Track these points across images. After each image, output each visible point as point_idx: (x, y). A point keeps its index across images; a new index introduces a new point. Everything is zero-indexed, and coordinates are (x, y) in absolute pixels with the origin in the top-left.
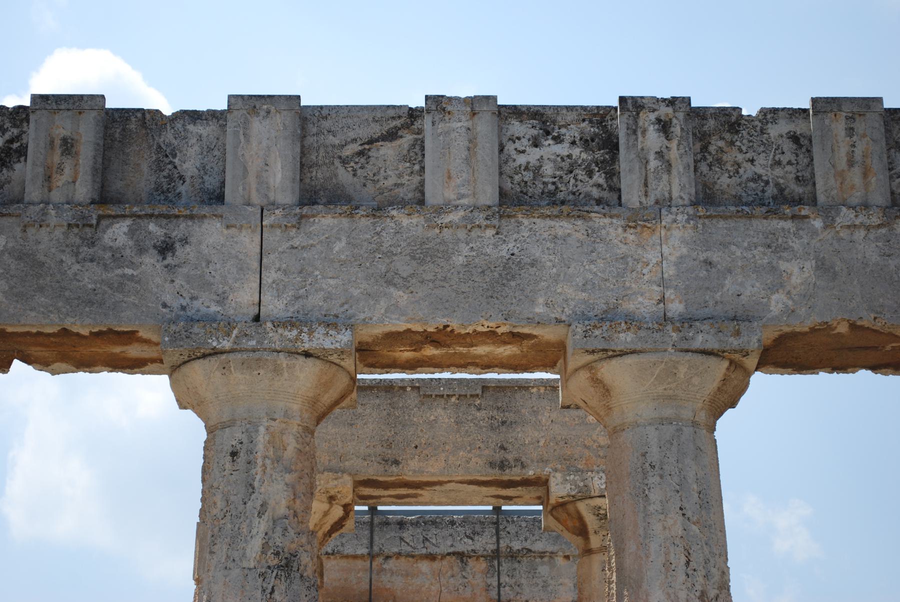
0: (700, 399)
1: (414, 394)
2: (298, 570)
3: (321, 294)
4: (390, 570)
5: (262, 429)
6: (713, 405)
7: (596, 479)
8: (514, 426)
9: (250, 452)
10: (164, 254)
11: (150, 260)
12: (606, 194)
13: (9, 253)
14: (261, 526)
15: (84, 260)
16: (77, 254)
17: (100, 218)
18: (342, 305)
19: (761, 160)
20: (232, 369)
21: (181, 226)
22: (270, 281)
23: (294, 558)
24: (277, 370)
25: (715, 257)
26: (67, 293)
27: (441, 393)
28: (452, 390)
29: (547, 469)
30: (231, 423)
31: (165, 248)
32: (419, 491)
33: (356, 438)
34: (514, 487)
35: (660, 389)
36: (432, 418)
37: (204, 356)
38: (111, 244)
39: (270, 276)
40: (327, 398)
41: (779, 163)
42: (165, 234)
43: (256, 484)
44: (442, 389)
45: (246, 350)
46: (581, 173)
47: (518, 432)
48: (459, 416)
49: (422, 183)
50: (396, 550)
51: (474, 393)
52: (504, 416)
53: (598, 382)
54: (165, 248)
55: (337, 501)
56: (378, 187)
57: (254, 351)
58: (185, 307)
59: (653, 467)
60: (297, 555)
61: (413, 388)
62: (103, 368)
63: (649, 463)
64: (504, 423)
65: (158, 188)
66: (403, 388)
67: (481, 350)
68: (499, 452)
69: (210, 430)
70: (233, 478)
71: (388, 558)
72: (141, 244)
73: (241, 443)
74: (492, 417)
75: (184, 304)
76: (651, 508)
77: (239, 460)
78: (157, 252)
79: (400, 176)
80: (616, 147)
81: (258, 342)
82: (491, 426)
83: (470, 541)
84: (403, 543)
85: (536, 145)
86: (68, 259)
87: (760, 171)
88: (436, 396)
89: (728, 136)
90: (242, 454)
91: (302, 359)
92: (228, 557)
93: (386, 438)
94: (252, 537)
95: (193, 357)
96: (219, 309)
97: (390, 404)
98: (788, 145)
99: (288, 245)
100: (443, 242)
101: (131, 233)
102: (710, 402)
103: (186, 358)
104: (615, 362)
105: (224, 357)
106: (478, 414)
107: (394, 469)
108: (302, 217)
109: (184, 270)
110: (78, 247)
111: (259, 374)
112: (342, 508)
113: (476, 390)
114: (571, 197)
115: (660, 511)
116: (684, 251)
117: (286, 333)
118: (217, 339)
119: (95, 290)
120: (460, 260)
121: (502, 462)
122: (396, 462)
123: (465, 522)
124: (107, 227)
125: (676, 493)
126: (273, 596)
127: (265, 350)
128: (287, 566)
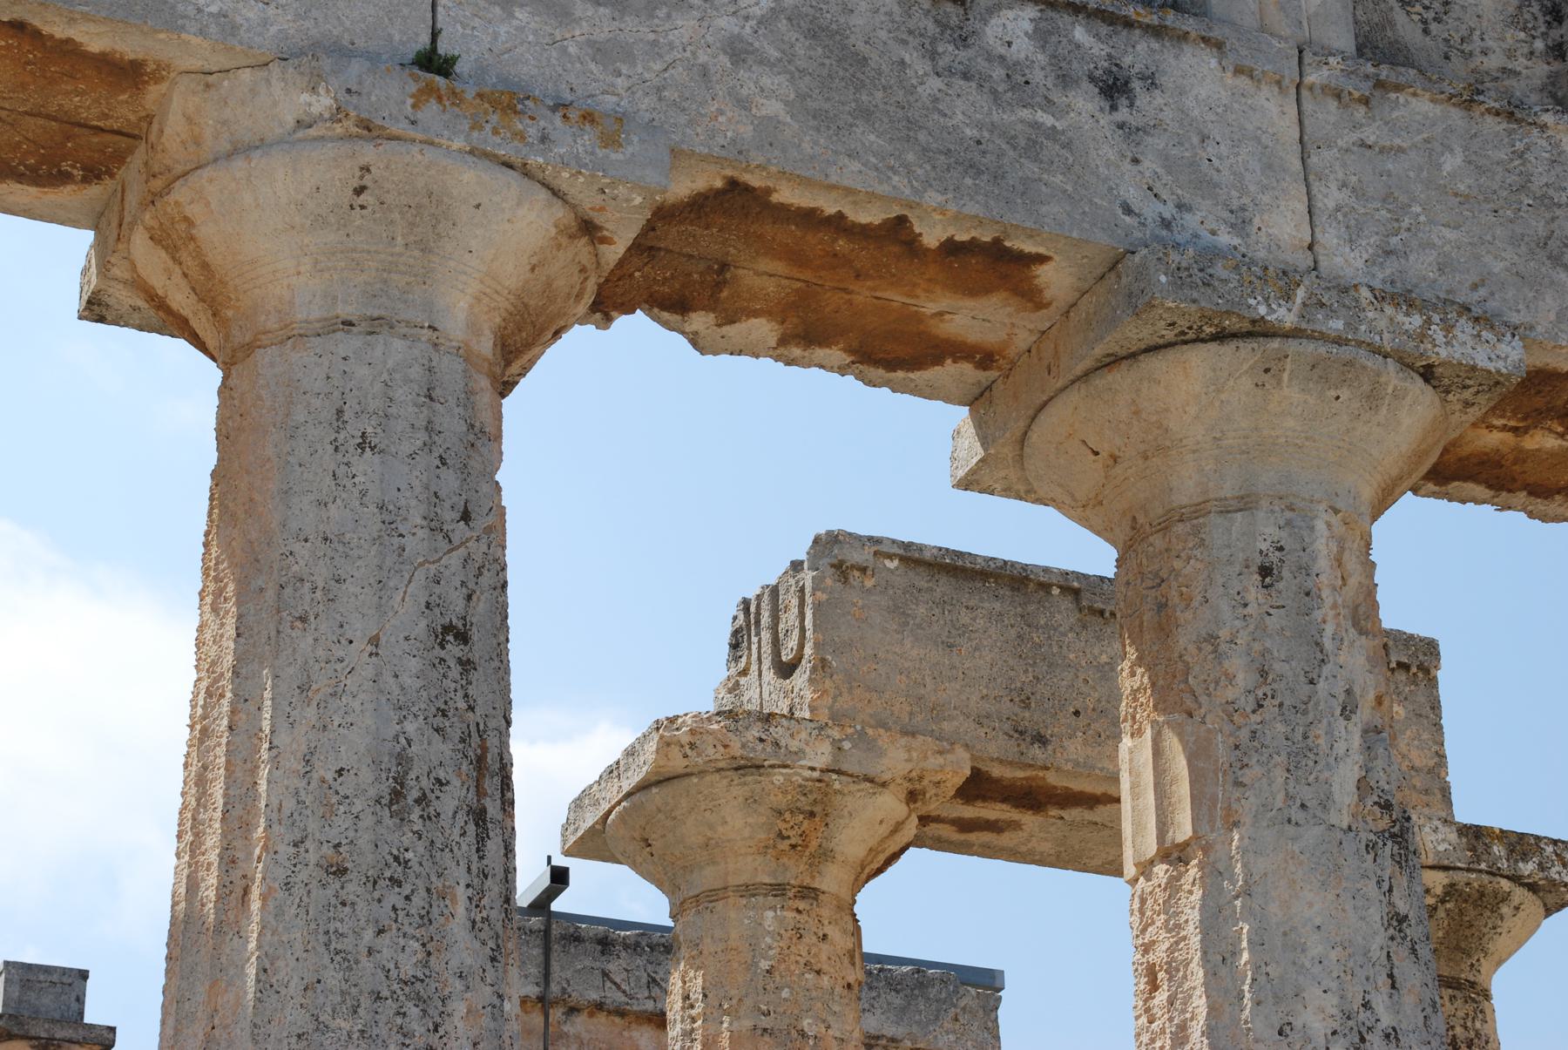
1: (1067, 603)
3: (1431, 256)
4: (578, 1037)
5: (1320, 525)
7: (1427, 829)
9: (1305, 570)
10: (1112, 97)
11: (1085, 103)
13: (789, 19)
15: (950, 71)
16: (933, 55)
18: (1475, 287)
20: (1286, 376)
21: (1139, 47)
22: (1331, 204)
24: (1373, 398)
26: (922, 136)
30: (1246, 503)
31: (1114, 88)
32: (1029, 819)
36: (1104, 658)
37: (1221, 337)
38: (1002, 50)
39: (1330, 197)
42: (1109, 56)
43: (1328, 644)
45: (1322, 337)
50: (594, 996)
56: (1472, 66)
57: (1339, 341)
58: (1170, 223)
61: (1066, 590)
66: (1045, 587)
70: (1273, 623)
71: (573, 1010)
72: (1063, 64)
73: (1281, 549)
75: (1167, 215)
77: (1281, 585)
78: (1097, 90)
79: (1510, 54)
81: (1347, 324)
84: (608, 984)
90: (1286, 573)
92: (1289, 797)
93: (1019, 685)
96: (1236, 241)
97: (1022, 616)
99: (1355, 136)
101: (1041, 36)
105: (1275, 344)
107: (1036, 751)
108: (1380, 84)
109: (1157, 142)
110: (934, 40)
111: (1338, 398)
117: (1400, 318)
118: (1267, 299)
119: (979, 142)
122: (1041, 740)
127: (1360, 344)
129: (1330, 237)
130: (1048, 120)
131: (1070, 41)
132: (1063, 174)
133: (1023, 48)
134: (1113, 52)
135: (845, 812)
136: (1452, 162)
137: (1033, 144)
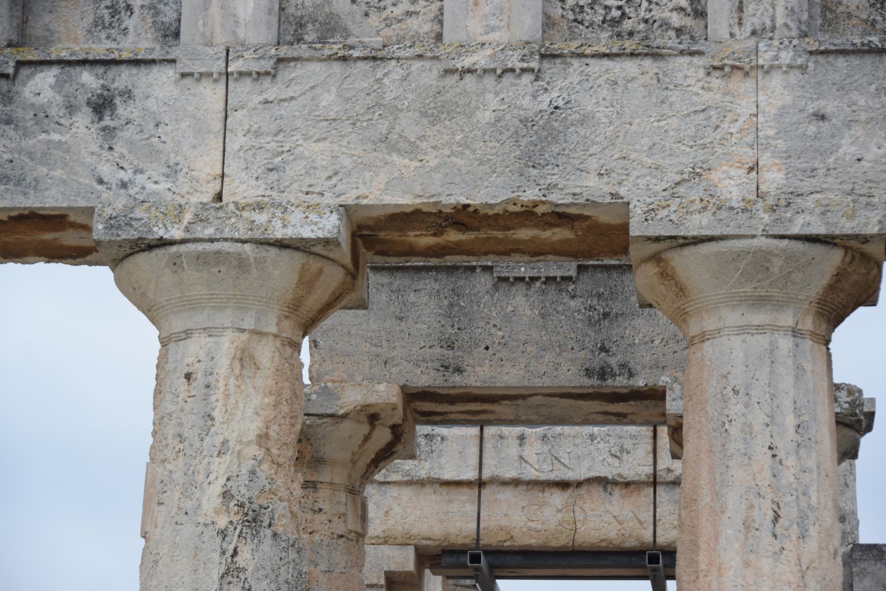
0: (805, 300)
2: (270, 525)
6: (825, 308)
8: (620, 319)
10: (100, 112)
11: (83, 119)
12: (689, 22)
14: (221, 467)
20: (185, 265)
21: (123, 75)
22: (236, 147)
23: (265, 511)
25: (829, 106)
27: (522, 275)
28: (536, 271)
29: (663, 378)
33: (407, 336)
34: (623, 401)
35: (748, 289)
36: (510, 309)
38: (33, 100)
40: (314, 300)
42: (103, 86)
44: (523, 269)
47: (625, 328)
48: (546, 306)
51: (567, 274)
52: (607, 305)
53: (669, 278)
55: (381, 420)
56: (384, 16)
57: (212, 240)
58: (127, 183)
59: (736, 392)
60: (269, 507)
62: (37, 258)
63: (732, 386)
64: (606, 315)
65: (98, 23)
67: (524, 234)
68: (599, 354)
69: (164, 342)
72: (72, 99)
74: (590, 307)
75: (126, 179)
76: (732, 447)
78: (91, 110)
82: (590, 319)
83: (616, 462)
84: (524, 465)
88: (516, 279)
91: (273, 251)
92: (180, 508)
93: (447, 336)
94: (209, 483)
95: (137, 249)
97: (453, 290)
99: (261, 98)
100: (465, 93)
101: (58, 86)
102: (819, 303)
103: (129, 251)
104: (687, 251)
105: (174, 249)
106: (571, 303)
108: (280, 60)
109: (128, 133)
111: (220, 271)
112: (389, 430)
113: (569, 270)
114: (642, 26)
115: (743, 451)
116: (788, 99)
118: (165, 225)
119: (11, 161)
120: (485, 116)
121: (602, 368)
122: (459, 370)
123: (610, 436)
124: (30, 77)
125: (765, 428)
126: (235, 559)
128: (254, 520)
129: (233, 167)
130: (55, 137)
131: (77, 84)
132: (62, 169)
134: (106, 84)
135: (319, 436)
136: (328, 99)
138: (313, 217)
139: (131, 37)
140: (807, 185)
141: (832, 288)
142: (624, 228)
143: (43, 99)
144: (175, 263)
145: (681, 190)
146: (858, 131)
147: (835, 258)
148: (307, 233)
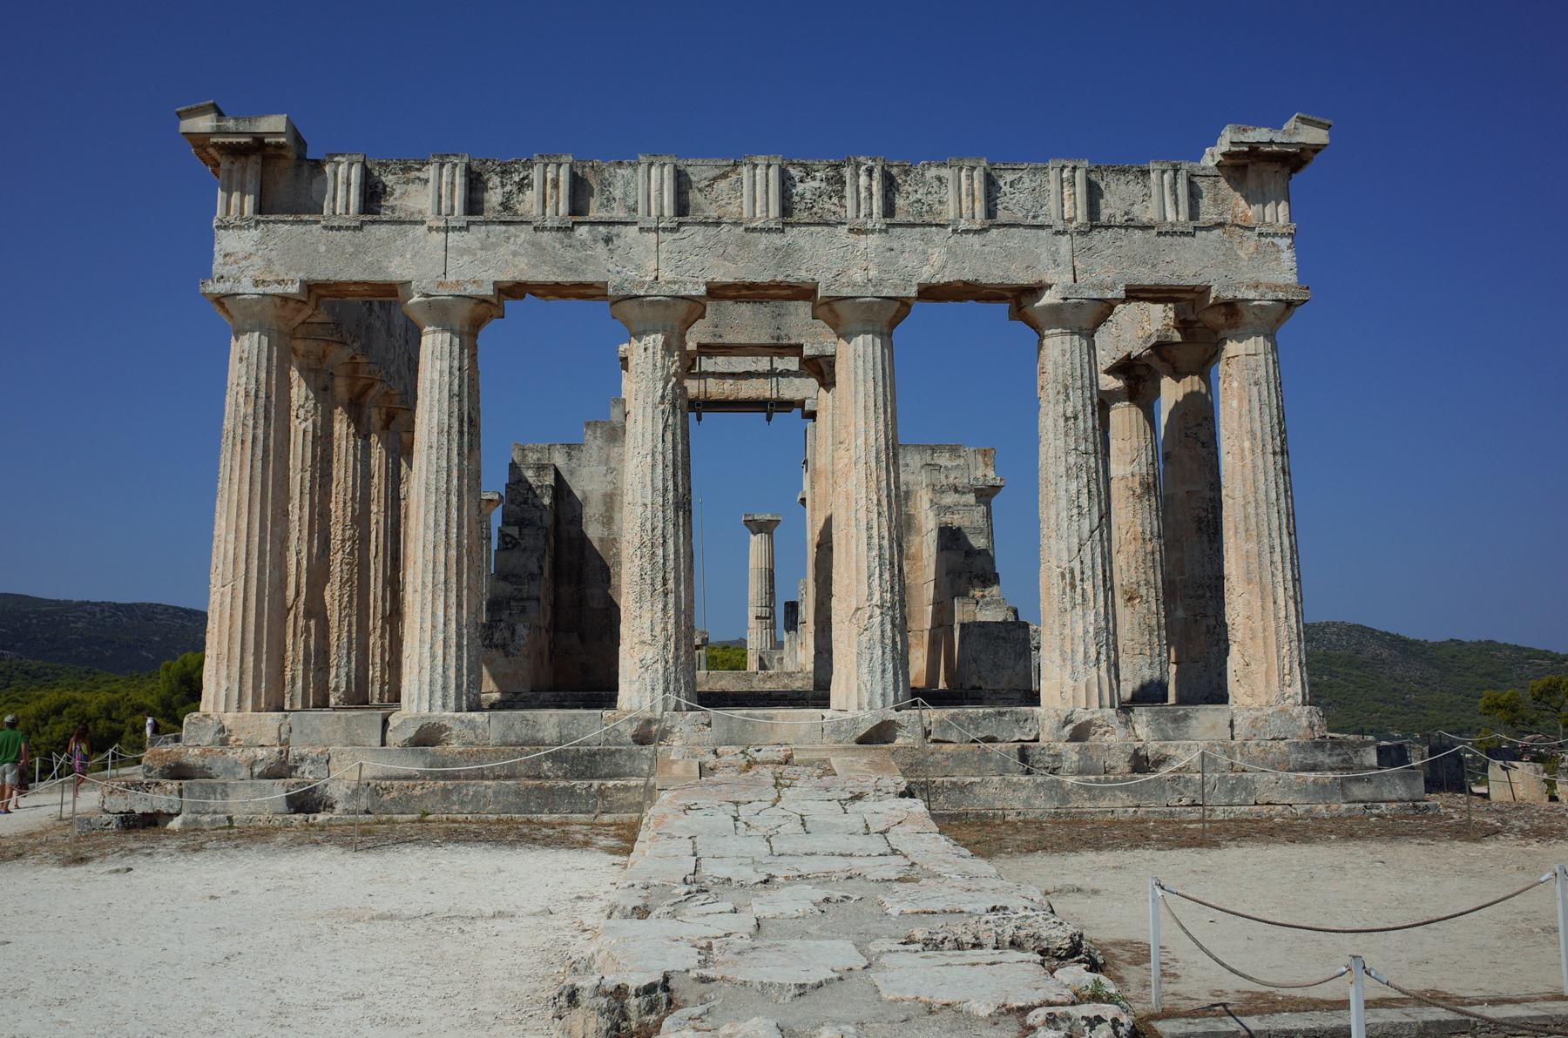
11: (601, 245)
12: (838, 209)
17: (574, 223)
19: (920, 191)
31: (608, 240)
39: (662, 257)
41: (930, 193)
46: (826, 199)
49: (742, 202)
54: (608, 240)
65: (602, 204)
67: (772, 292)
80: (845, 182)
85: (801, 181)
86: (558, 246)
87: (919, 196)
89: (903, 176)
98: (935, 183)
101: (590, 232)
104: (841, 302)
109: (619, 251)
120: (761, 247)
122: (721, 336)
130: (590, 253)
133: (585, 235)
136: (699, 239)
137: (586, 261)
138: (696, 287)
139: (615, 211)
140: (886, 276)
141: (895, 316)
142: (815, 291)
143: (582, 238)
144: (641, 304)
145: (838, 278)
146: (906, 255)
147: (898, 304)
148: (694, 293)
